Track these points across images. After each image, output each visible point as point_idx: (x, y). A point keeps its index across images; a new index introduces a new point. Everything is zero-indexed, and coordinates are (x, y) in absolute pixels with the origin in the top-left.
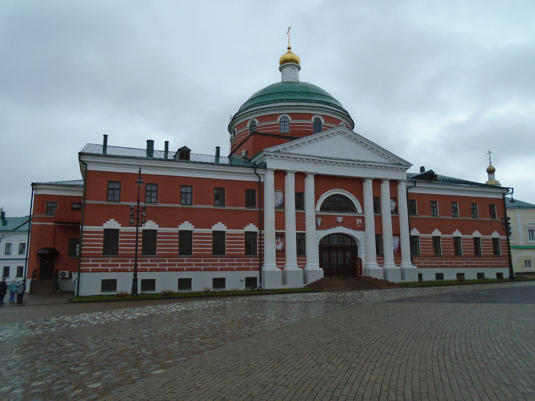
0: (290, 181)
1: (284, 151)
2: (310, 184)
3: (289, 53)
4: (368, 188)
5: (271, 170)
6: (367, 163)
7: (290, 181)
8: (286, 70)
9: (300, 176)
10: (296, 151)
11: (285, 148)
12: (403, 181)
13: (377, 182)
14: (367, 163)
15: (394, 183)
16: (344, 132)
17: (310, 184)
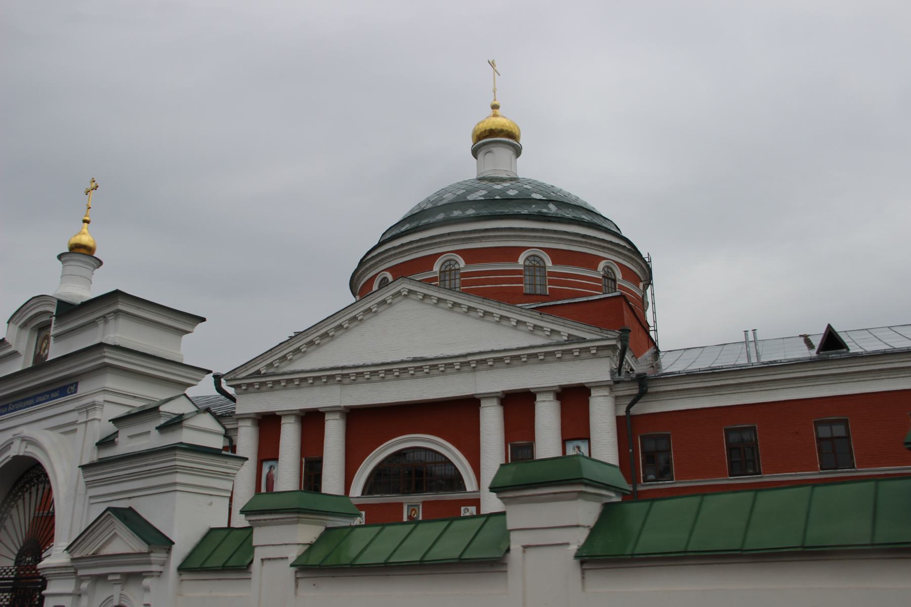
0: (290, 436)
1: (272, 370)
2: (334, 433)
3: (495, 115)
4: (491, 420)
5: (244, 417)
6: (470, 358)
7: (290, 436)
8: (480, 156)
9: (312, 421)
11: (271, 364)
12: (599, 385)
13: (518, 405)
14: (470, 358)
15: (573, 399)
16: (410, 291)
17: (334, 433)
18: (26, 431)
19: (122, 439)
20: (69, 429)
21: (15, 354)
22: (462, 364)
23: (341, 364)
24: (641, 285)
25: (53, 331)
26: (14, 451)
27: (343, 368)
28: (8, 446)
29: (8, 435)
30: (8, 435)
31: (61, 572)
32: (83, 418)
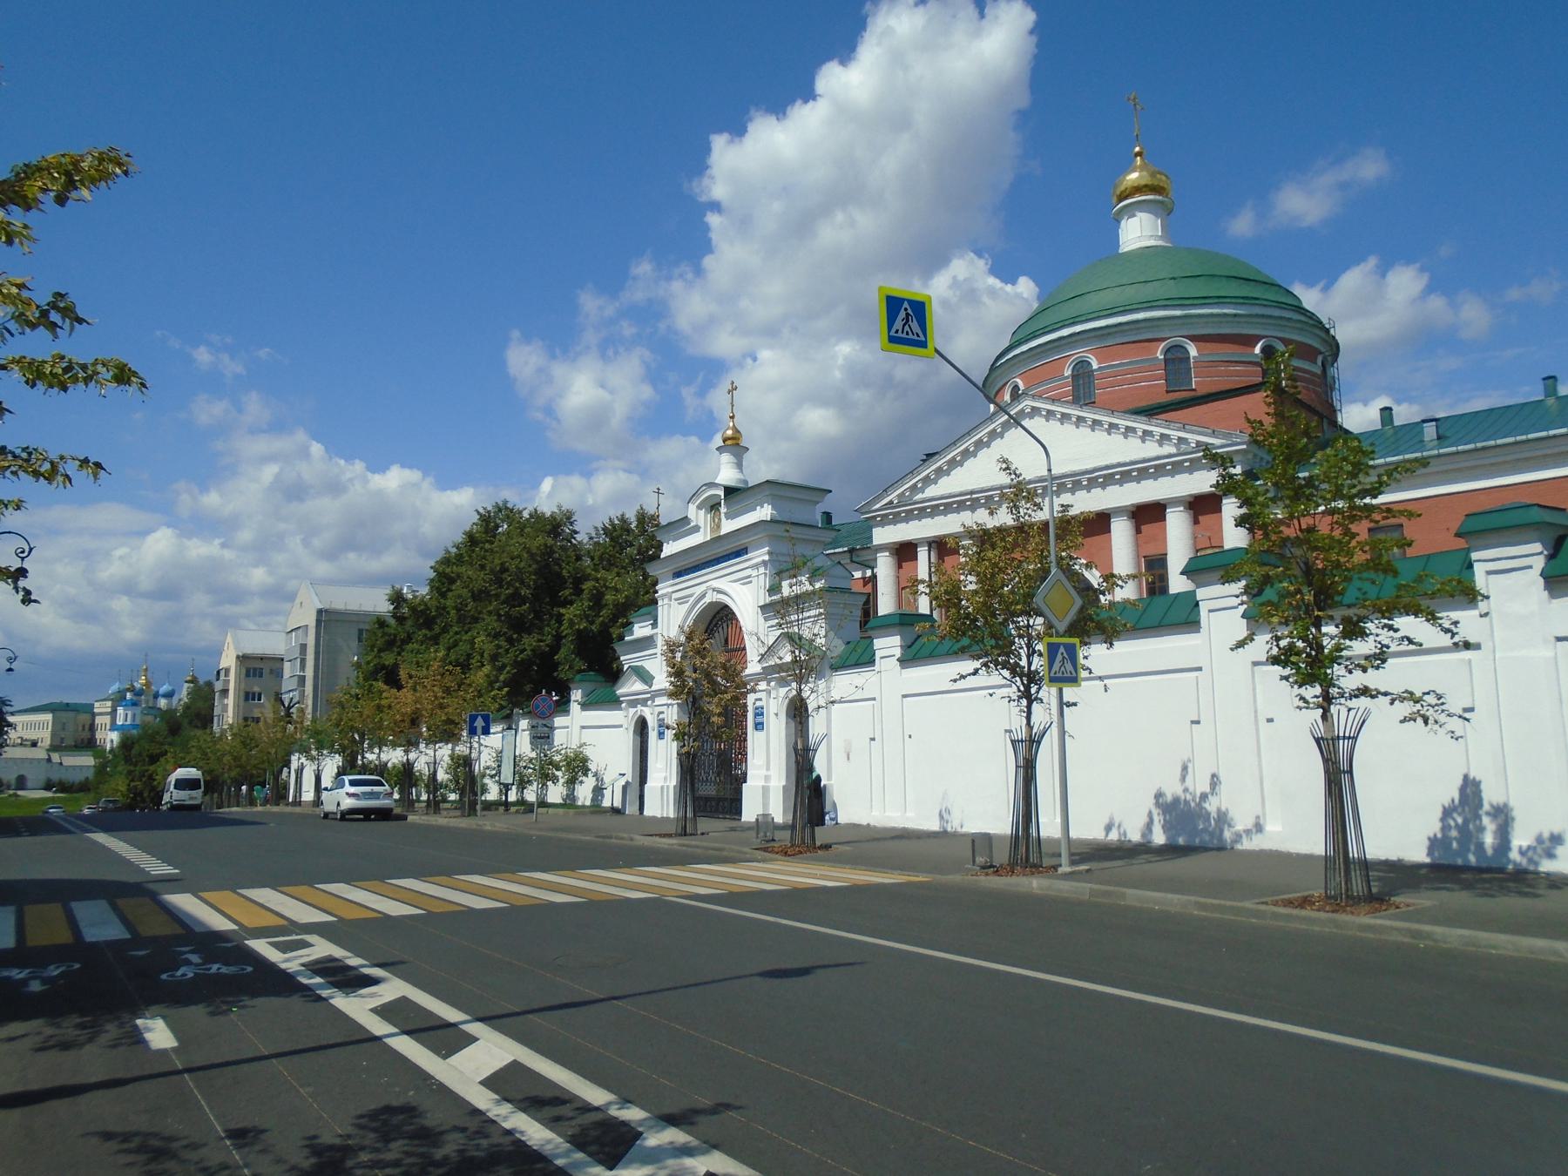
5: (882, 548)
10: (931, 491)
13: (1148, 515)
16: (1033, 408)
18: (715, 584)
19: (785, 584)
20: (746, 581)
21: (696, 529)
22: (1089, 480)
23: (970, 488)
24: (1320, 359)
25: (723, 509)
26: (707, 600)
27: (972, 493)
28: (703, 596)
29: (703, 588)
30: (703, 588)
31: (758, 678)
32: (755, 573)
